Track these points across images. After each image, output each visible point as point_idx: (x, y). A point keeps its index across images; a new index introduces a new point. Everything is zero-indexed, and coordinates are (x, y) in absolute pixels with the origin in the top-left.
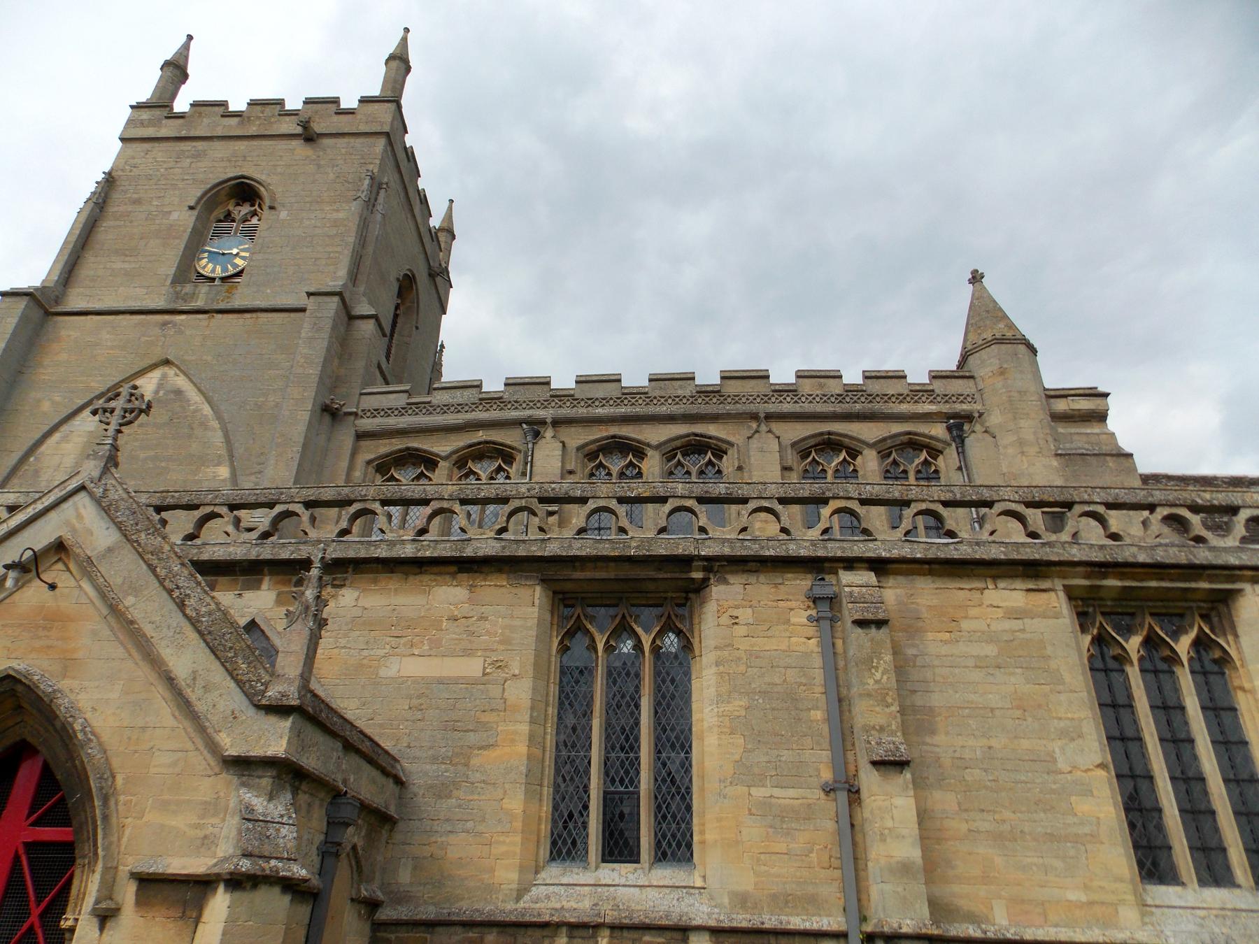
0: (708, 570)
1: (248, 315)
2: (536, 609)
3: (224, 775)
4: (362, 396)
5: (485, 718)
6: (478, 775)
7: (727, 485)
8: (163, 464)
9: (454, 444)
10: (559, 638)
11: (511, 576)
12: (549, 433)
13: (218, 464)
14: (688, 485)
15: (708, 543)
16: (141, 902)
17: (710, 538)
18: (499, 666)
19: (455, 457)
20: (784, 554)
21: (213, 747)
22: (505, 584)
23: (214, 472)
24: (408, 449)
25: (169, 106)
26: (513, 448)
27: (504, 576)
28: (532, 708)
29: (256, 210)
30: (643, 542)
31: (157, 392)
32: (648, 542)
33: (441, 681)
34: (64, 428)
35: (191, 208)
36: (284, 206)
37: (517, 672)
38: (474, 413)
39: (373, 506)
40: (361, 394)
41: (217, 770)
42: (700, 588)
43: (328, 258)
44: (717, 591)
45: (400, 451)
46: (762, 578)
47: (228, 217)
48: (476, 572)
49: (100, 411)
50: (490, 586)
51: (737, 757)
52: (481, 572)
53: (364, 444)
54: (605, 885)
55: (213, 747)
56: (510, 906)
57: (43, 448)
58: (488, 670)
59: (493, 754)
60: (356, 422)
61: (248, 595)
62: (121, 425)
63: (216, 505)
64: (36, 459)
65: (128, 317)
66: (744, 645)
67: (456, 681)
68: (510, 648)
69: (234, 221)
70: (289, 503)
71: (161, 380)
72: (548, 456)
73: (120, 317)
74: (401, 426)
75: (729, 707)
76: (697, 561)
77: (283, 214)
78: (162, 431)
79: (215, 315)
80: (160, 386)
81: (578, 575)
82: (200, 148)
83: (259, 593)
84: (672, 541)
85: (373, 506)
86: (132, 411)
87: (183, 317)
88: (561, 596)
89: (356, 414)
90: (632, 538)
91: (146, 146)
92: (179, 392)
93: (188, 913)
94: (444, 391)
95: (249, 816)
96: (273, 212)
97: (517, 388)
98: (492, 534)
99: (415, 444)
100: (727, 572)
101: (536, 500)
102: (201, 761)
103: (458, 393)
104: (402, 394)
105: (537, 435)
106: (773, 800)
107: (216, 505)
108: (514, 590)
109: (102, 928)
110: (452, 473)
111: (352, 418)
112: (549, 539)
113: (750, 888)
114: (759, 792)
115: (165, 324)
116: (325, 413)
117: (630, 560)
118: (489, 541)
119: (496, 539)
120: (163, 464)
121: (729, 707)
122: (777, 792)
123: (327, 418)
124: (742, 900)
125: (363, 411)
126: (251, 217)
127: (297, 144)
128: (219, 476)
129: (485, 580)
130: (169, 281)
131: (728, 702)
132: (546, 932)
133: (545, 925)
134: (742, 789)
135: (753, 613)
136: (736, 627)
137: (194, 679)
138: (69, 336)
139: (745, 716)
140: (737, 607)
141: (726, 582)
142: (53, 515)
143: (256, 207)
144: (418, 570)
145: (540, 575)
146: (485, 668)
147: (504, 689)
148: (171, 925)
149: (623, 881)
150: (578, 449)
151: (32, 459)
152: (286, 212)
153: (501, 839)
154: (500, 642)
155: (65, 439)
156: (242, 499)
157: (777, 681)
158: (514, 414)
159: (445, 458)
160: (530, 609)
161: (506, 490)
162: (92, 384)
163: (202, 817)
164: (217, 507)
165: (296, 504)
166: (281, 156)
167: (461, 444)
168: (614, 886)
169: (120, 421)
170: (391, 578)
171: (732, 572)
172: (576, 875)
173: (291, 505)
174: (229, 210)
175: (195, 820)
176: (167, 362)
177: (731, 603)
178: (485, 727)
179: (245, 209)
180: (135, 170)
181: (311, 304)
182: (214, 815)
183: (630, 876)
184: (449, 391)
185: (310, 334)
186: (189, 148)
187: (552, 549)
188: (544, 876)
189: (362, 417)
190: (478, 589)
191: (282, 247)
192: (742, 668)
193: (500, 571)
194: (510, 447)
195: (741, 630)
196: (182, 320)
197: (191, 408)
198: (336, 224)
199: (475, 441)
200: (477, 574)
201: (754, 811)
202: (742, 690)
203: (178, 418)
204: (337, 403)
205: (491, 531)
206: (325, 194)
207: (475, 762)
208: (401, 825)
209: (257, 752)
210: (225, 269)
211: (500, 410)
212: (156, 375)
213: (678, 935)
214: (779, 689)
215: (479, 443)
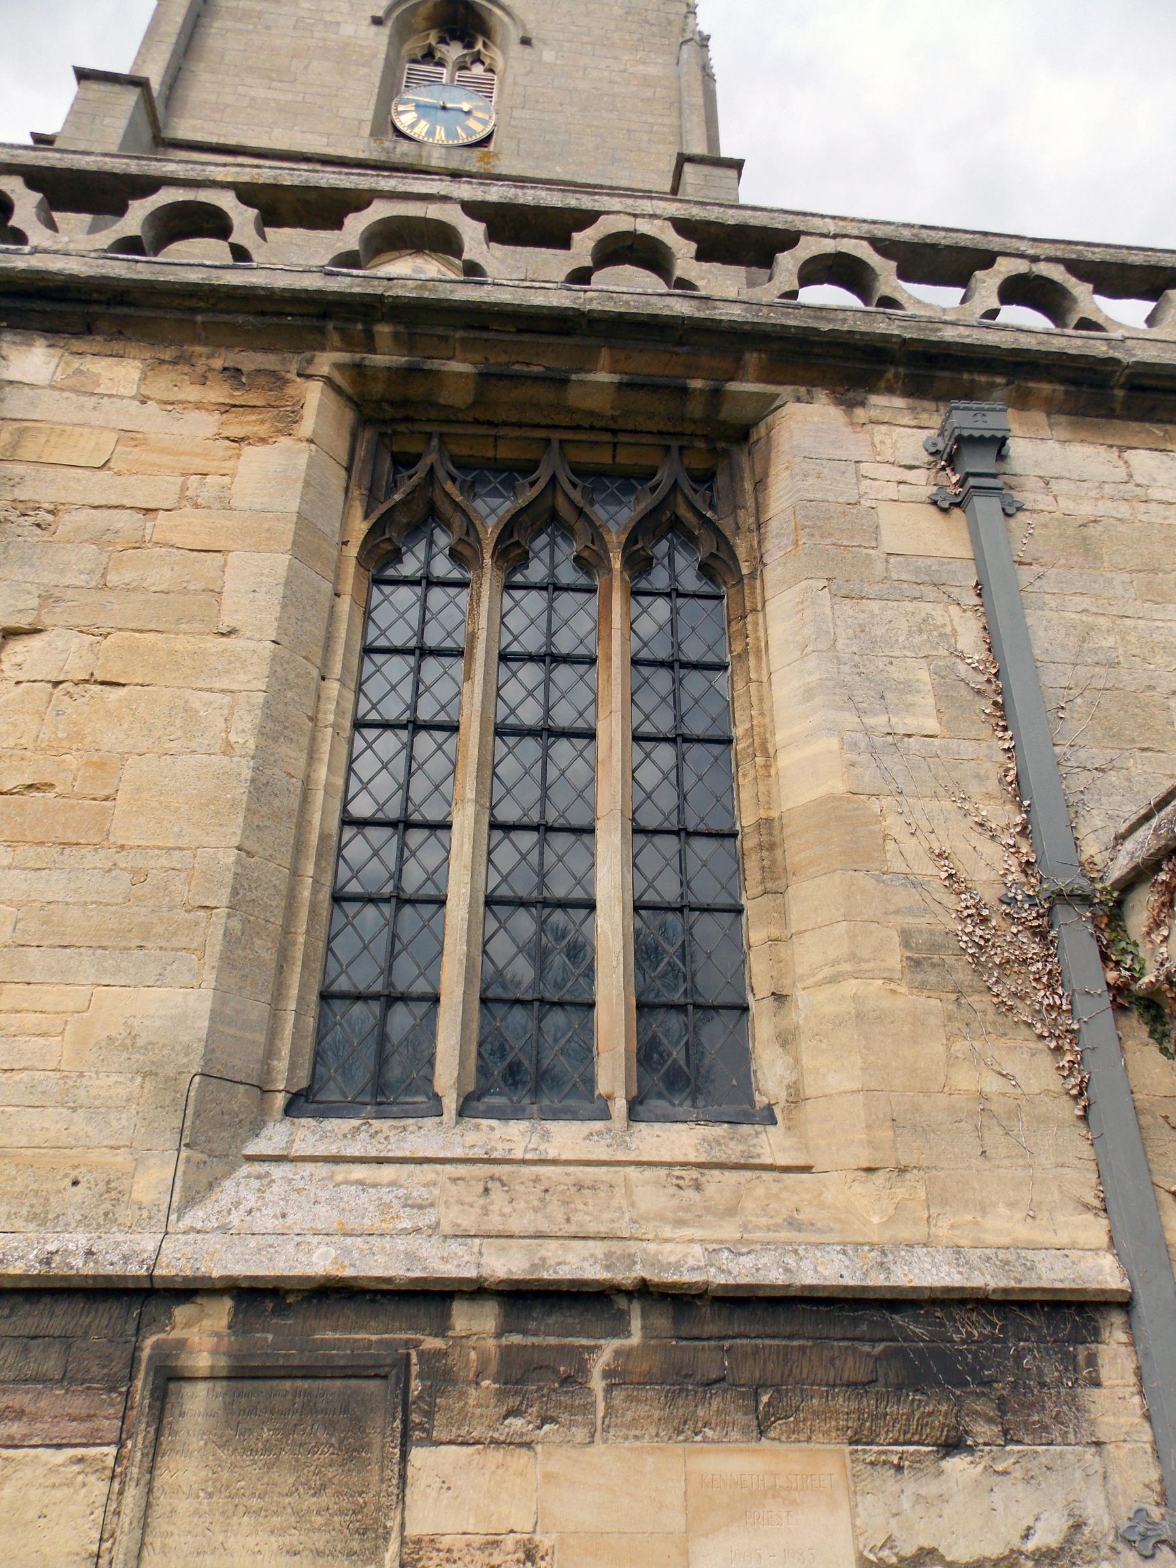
29: (479, 52)
35: (377, 21)
36: (545, 44)
43: (651, 132)
69: (441, 63)
77: (548, 56)
96: (527, 49)
126: (473, 63)
130: (366, 131)
174: (430, 45)
198: (646, 81)
206: (616, 36)
210: (451, 133)
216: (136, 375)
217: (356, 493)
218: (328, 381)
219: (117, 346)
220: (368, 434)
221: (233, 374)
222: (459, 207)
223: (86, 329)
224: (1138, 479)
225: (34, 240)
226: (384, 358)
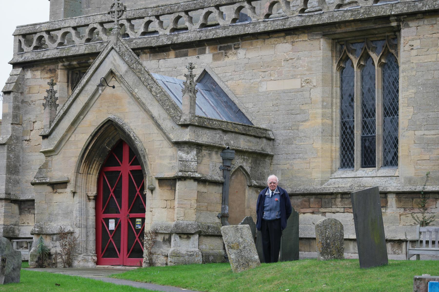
0: (398, 20)
2: (321, 51)
3: (174, 147)
5: (303, 107)
6: (302, 134)
10: (337, 63)
11: (310, 34)
15: (398, 5)
16: (160, 185)
17: (398, 3)
18: (308, 82)
20: (432, 8)
21: (169, 139)
22: (307, 39)
27: (306, 35)
28: (323, 101)
30: (366, 9)
32: (369, 9)
33: (284, 92)
37: (315, 84)
39: (244, 4)
41: (172, 146)
42: (398, 30)
44: (404, 32)
46: (426, 22)
48: (293, 34)
49: (111, 13)
50: (300, 41)
51: (410, 117)
52: (296, 34)
54: (358, 177)
55: (169, 139)
56: (319, 187)
58: (303, 85)
59: (307, 124)
61: (201, 57)
62: (118, 18)
63: (179, 12)
66: (415, 60)
67: (290, 91)
68: (311, 72)
70: (209, 7)
75: (408, 93)
76: (392, 17)
81: (339, 30)
83: (205, 55)
84: (380, 7)
85: (244, 4)
86: (120, 11)
88: (336, 41)
90: (361, 7)
93: (172, 188)
95: (181, 160)
98: (297, 14)
100: (409, 21)
102: (166, 143)
106: (425, 136)
107: (179, 12)
108: (312, 42)
109: (152, 193)
112: (323, 13)
113: (413, 175)
114: (419, 133)
117: (361, 21)
118: (297, 17)
119: (299, 16)
121: (408, 93)
122: (426, 132)
124: (409, 180)
129: (298, 38)
131: (407, 91)
132: (333, 196)
133: (332, 194)
134: (411, 132)
135: (421, 42)
136: (412, 51)
137: (160, 117)
139: (414, 98)
140: (413, 40)
141: (408, 26)
142: (106, 59)
144: (268, 37)
145: (322, 32)
146: (302, 84)
147: (310, 93)
148: (169, 192)
149: (366, 175)
153: (314, 160)
154: (307, 70)
156: (189, 7)
157: (430, 78)
160: (319, 52)
163: (171, 160)
164: (180, 13)
165: (212, 7)
168: (362, 177)
169: (118, 16)
170: (258, 42)
171: (411, 20)
172: (348, 173)
173: (210, 8)
175: (169, 161)
177: (410, 38)
178: (303, 112)
182: (174, 160)
183: (370, 173)
187: (325, 19)
188: (336, 175)
190: (295, 43)
192: (414, 73)
193: (304, 33)
195: (414, 52)
200: (294, 36)
201: (416, 142)
202: (414, 84)
205: (297, 12)
207: (301, 128)
208: (275, 157)
209: (180, 140)
213: (383, 196)
214: (430, 82)
216: (40, 74)
217: (70, 85)
218: (61, 69)
219: (37, 68)
220: (70, 72)
221: (50, 70)
222: (71, 28)
223: (33, 66)
224: (160, 67)
225: (25, 51)
226: (66, 63)
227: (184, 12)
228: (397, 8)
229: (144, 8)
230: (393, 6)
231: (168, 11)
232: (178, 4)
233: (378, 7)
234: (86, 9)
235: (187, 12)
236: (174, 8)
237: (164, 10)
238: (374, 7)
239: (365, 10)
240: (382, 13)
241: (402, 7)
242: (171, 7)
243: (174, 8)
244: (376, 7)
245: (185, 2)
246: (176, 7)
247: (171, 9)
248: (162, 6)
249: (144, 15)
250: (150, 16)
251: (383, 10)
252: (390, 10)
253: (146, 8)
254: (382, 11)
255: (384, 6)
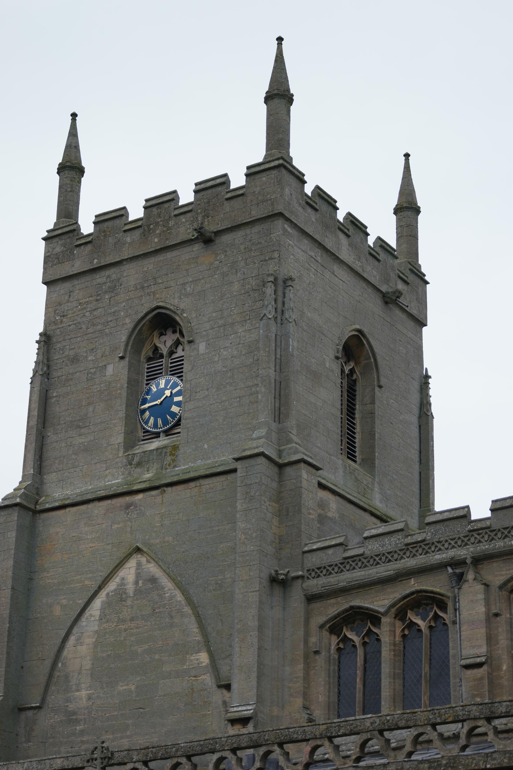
1: (192, 484)
4: (305, 555)
7: (508, 703)
8: (157, 657)
9: (392, 596)
12: (470, 576)
13: (199, 651)
14: (480, 707)
15: (495, 755)
17: (495, 752)
19: (393, 610)
23: (197, 660)
24: (352, 607)
25: (75, 230)
26: (442, 595)
30: (450, 760)
31: (136, 583)
32: (453, 759)
34: (75, 630)
35: (122, 358)
38: (403, 561)
39: (274, 748)
40: (304, 552)
45: (346, 610)
47: (156, 352)
49: (91, 761)
53: (316, 606)
57: (65, 653)
60: (304, 585)
63: (178, 757)
64: (62, 664)
65: (97, 504)
70: (222, 751)
71: (137, 569)
72: (472, 601)
73: (91, 506)
74: (342, 584)
77: (202, 347)
78: (149, 623)
79: (165, 489)
80: (138, 576)
82: (114, 276)
84: (470, 757)
85: (274, 748)
86: (105, 758)
87: (140, 496)
89: (302, 577)
90: (443, 757)
91: (67, 285)
92: (153, 580)
94: (374, 539)
96: (193, 346)
97: (438, 526)
99: (357, 602)
101: (377, 732)
103: (386, 540)
104: (338, 548)
105: (460, 578)
107: (178, 757)
110: (395, 626)
111: (300, 581)
115: (128, 506)
116: (274, 584)
119: (354, 767)
120: (157, 657)
123: (278, 590)
125: (308, 571)
126: (176, 348)
127: (197, 247)
128: (202, 663)
130: (122, 450)
138: (57, 533)
143: (178, 335)
150: (501, 587)
151: (60, 665)
152: (204, 343)
155: (79, 642)
156: (193, 750)
158: (438, 557)
159: (385, 614)
161: (357, 726)
162: (87, 582)
164: (179, 758)
165: (226, 752)
166: (187, 270)
167: (398, 596)
169: (101, 766)
173: (223, 752)
176: (138, 550)
179: (170, 339)
180: (64, 320)
181: (238, 465)
184: (378, 538)
185: (245, 506)
186: (104, 280)
189: (308, 578)
191: (208, 389)
194: (439, 594)
196: (140, 500)
197: (167, 595)
199: (408, 592)
203: (159, 608)
204: (281, 574)
205: (350, 761)
211: (425, 554)
212: (132, 563)
215: (412, 593)
227: (185, 757)
228: (494, 759)
229: (126, 751)
230: (487, 757)
231: (162, 755)
232: (176, 746)
233: (466, 757)
234: (25, 745)
235: (189, 758)
236: (171, 752)
237: (155, 753)
238: (461, 757)
239: (448, 761)
240: (473, 765)
241: (501, 758)
242: (166, 749)
243: (171, 752)
244: (464, 757)
245: (187, 743)
246: (174, 749)
247: (167, 753)
248: (153, 748)
249: (126, 761)
250: (135, 762)
251: (474, 762)
252: (484, 761)
253: (129, 750)
254: (472, 763)
255: (476, 756)
